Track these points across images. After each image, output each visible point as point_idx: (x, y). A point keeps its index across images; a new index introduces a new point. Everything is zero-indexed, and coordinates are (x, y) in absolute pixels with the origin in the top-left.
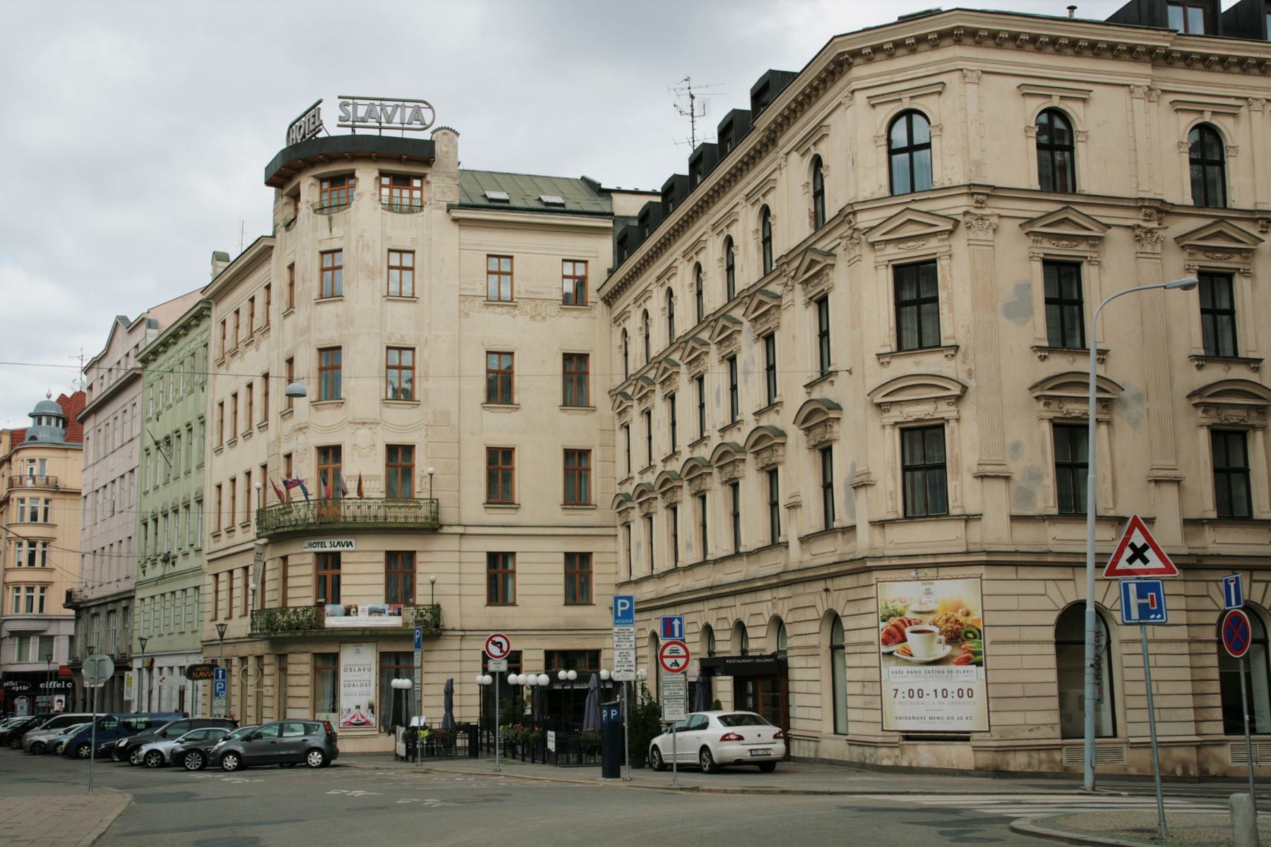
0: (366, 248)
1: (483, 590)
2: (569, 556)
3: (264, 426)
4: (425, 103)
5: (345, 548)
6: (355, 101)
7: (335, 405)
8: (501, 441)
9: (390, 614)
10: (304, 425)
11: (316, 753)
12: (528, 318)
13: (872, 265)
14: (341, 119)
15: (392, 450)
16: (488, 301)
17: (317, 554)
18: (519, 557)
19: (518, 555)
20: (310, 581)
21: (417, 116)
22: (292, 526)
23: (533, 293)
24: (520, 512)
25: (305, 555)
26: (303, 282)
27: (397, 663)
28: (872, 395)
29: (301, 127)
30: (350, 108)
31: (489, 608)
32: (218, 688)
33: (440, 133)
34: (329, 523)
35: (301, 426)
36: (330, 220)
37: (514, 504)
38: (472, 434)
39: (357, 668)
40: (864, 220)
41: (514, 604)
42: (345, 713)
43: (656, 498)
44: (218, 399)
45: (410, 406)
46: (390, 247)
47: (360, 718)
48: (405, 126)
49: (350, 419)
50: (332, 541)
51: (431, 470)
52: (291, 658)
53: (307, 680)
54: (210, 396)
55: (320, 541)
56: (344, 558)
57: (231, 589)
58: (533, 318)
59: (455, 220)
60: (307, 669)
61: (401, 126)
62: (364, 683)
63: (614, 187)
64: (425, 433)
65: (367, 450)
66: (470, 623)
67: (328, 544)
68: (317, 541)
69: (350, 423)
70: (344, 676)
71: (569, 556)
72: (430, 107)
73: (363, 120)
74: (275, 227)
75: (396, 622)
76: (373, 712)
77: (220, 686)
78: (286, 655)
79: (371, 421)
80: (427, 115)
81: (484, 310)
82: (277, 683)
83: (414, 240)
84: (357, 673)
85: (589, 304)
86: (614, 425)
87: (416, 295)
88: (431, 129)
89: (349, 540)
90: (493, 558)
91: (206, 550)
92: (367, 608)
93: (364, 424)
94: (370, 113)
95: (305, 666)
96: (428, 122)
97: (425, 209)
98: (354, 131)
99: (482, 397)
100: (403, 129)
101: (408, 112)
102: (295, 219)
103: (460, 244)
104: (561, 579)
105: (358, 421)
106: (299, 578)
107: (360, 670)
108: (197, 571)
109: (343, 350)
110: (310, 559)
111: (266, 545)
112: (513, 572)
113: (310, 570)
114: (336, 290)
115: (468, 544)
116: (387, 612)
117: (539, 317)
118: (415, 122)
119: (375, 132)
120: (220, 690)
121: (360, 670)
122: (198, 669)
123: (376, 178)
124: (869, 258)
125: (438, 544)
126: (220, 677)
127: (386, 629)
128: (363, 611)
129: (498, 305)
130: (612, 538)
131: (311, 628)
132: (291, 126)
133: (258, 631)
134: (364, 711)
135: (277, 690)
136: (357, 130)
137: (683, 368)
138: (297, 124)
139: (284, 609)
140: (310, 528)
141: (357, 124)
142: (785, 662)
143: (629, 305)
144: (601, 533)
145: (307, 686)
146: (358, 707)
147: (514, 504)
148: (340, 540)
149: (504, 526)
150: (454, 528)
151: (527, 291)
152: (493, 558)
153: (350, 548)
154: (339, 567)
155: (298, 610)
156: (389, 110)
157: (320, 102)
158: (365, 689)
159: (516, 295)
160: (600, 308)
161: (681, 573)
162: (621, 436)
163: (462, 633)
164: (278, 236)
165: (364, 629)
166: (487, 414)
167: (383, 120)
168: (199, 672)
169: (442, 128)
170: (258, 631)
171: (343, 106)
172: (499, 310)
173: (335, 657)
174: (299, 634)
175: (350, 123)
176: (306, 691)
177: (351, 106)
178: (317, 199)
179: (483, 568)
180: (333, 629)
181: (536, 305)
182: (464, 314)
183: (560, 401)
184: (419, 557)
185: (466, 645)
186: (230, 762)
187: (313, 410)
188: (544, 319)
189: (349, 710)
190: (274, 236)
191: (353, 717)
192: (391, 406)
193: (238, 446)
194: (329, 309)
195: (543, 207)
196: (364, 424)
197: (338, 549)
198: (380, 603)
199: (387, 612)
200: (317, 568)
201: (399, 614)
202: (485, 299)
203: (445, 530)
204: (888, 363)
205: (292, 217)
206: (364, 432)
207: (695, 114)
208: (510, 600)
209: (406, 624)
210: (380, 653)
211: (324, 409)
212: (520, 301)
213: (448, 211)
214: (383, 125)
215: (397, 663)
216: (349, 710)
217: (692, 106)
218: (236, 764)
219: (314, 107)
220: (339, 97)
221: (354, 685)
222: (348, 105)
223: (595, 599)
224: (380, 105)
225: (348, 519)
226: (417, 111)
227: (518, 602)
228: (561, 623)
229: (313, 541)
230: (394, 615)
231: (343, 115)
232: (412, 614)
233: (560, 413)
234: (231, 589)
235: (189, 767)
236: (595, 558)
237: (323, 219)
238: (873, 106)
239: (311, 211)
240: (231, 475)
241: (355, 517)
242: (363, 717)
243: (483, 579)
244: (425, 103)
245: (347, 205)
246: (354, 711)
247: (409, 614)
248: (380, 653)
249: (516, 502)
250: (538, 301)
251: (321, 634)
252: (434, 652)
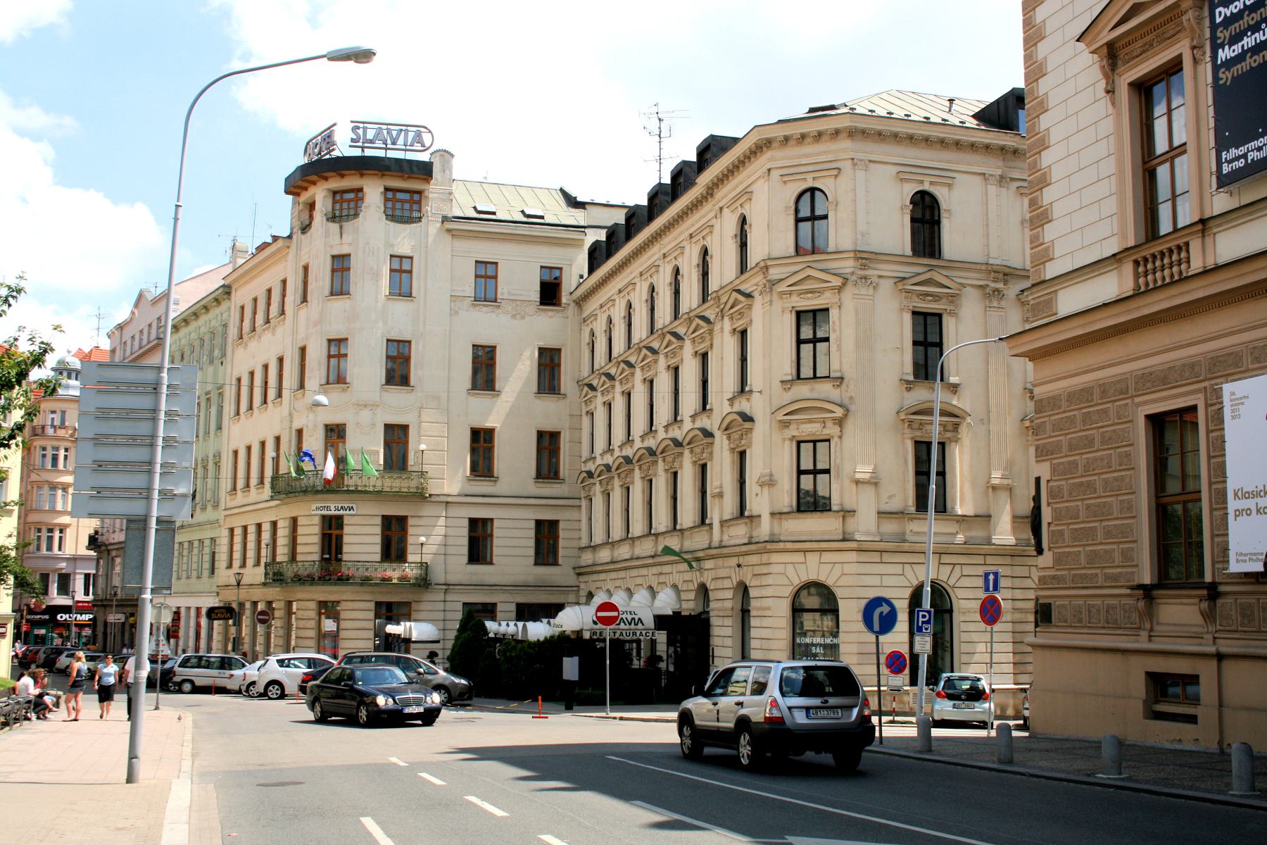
0: (371, 254)
1: (465, 550)
2: (539, 523)
4: (426, 128)
5: (348, 512)
6: (365, 125)
12: (509, 316)
13: (780, 310)
14: (353, 140)
15: (388, 427)
16: (475, 301)
17: (324, 517)
18: (496, 523)
19: (495, 521)
20: (316, 539)
21: (418, 138)
23: (513, 294)
24: (499, 484)
26: (316, 281)
28: (775, 414)
29: (317, 144)
30: (360, 132)
33: (438, 154)
36: (341, 227)
37: (493, 477)
40: (775, 273)
43: (614, 477)
44: (236, 375)
46: (392, 253)
48: (408, 148)
54: (229, 371)
58: (514, 316)
59: (449, 231)
61: (404, 147)
63: (588, 200)
66: (452, 579)
67: (333, 508)
69: (354, 404)
71: (539, 523)
72: (430, 132)
73: (371, 142)
74: (292, 229)
79: (372, 403)
80: (427, 138)
81: (472, 309)
83: (413, 247)
85: (563, 305)
86: (581, 411)
87: (413, 295)
88: (432, 150)
89: (351, 505)
90: (473, 523)
91: (222, 506)
93: (365, 406)
94: (377, 136)
96: (427, 145)
97: (423, 220)
98: (363, 151)
99: (467, 383)
100: (406, 150)
101: (411, 135)
102: (309, 225)
103: (452, 251)
104: (532, 543)
108: (214, 523)
109: (349, 342)
112: (491, 535)
114: (344, 288)
115: (454, 511)
117: (518, 316)
118: (416, 144)
119: (381, 153)
122: (216, 611)
123: (382, 193)
124: (778, 305)
125: (428, 510)
129: (484, 306)
132: (308, 143)
136: (365, 150)
137: (638, 373)
138: (314, 141)
141: (366, 145)
142: (708, 620)
143: (595, 309)
145: (313, 629)
147: (493, 477)
149: (484, 496)
151: (509, 293)
152: (473, 523)
153: (352, 512)
156: (394, 133)
157: (335, 125)
159: (499, 296)
160: (572, 308)
162: (586, 421)
163: (446, 587)
164: (295, 237)
167: (389, 142)
168: (217, 614)
169: (438, 151)
171: (355, 129)
172: (485, 309)
175: (360, 144)
177: (361, 130)
178: (330, 209)
181: (517, 305)
182: (454, 312)
183: (535, 389)
184: (411, 522)
185: (449, 598)
188: (523, 317)
190: (290, 237)
194: (339, 304)
195: (525, 220)
196: (365, 406)
197: (342, 512)
200: (323, 529)
202: (473, 299)
203: (433, 499)
204: (789, 388)
205: (307, 222)
206: (366, 415)
207: (662, 136)
208: (488, 559)
212: (503, 301)
213: (443, 222)
214: (388, 146)
217: (660, 128)
219: (329, 128)
220: (352, 122)
222: (358, 128)
223: (560, 561)
224: (387, 129)
226: (419, 134)
227: (494, 561)
228: (530, 580)
231: (355, 137)
236: (562, 525)
237: (334, 227)
238: (785, 182)
239: (325, 220)
240: (247, 442)
243: (465, 541)
244: (426, 128)
245: (356, 215)
249: (495, 475)
250: (518, 303)
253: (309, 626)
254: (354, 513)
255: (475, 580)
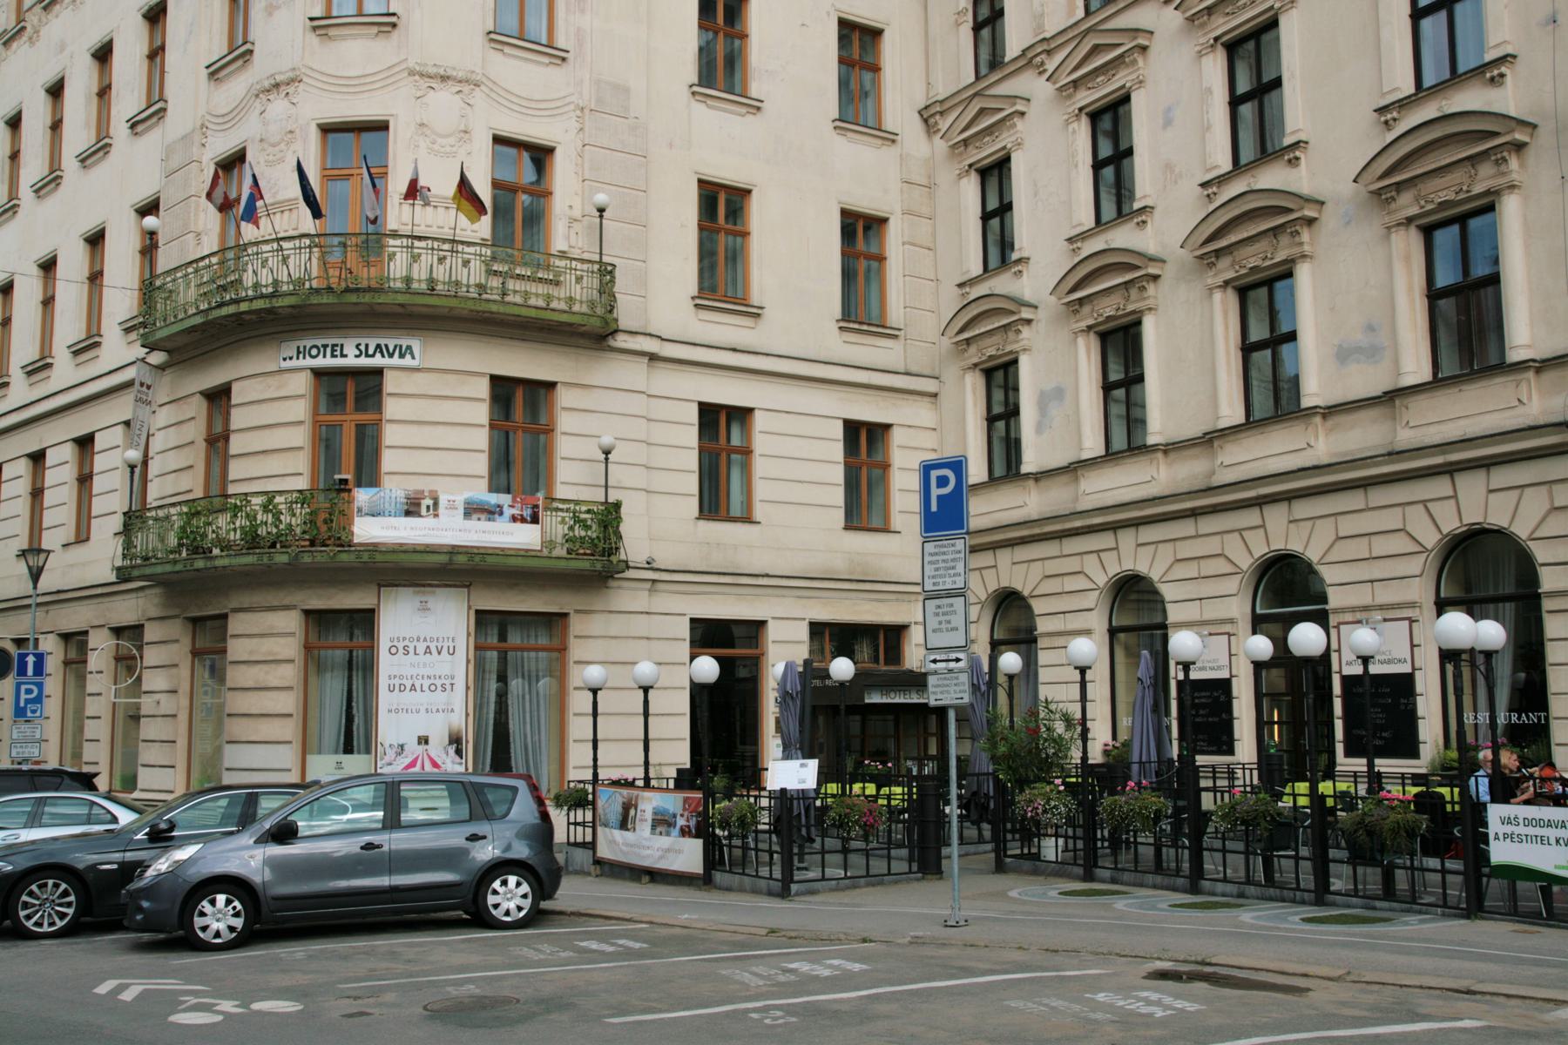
2: (852, 429)
3: (153, 112)
5: (396, 361)
7: (375, 29)
8: (727, 172)
9: (514, 519)
10: (291, 75)
11: (512, 880)
17: (318, 373)
20: (300, 437)
22: (263, 296)
24: (764, 324)
25: (287, 375)
27: (503, 637)
31: (702, 523)
32: (23, 697)
34: (369, 289)
35: (279, 78)
38: (671, 146)
39: (421, 647)
41: (747, 519)
42: (391, 754)
45: (546, 60)
47: (428, 767)
49: (411, 63)
50: (363, 341)
51: (601, 198)
52: (236, 624)
53: (289, 674)
55: (330, 342)
56: (391, 383)
57: (37, 493)
60: (290, 648)
62: (438, 683)
64: (578, 126)
65: (452, 140)
66: (665, 558)
67: (350, 350)
68: (319, 343)
69: (412, 73)
70: (387, 666)
71: (852, 429)
75: (525, 537)
76: (459, 752)
77: (29, 691)
78: (224, 617)
79: (461, 75)
82: (185, 687)
84: (422, 658)
92: (460, 499)
93: (444, 78)
95: (282, 640)
105: (433, 71)
106: (267, 432)
107: (428, 651)
110: (301, 384)
111: (161, 368)
112: (747, 452)
113: (300, 410)
116: (508, 512)
120: (27, 701)
121: (428, 651)
126: (30, 671)
127: (503, 553)
128: (452, 506)
130: (928, 399)
131: (313, 543)
133: (139, 561)
134: (439, 750)
135: (185, 702)
139: (218, 498)
140: (315, 300)
144: (912, 387)
145: (289, 688)
146: (424, 740)
148: (382, 342)
150: (640, 339)
152: (713, 418)
153: (408, 361)
154: (378, 407)
155: (279, 499)
158: (440, 698)
161: (1318, 419)
165: (454, 550)
166: (699, 109)
170: (139, 561)
173: (365, 621)
174: (281, 559)
176: (288, 703)
179: (690, 436)
180: (374, 548)
184: (564, 398)
186: (219, 916)
187: (313, 39)
189: (402, 747)
191: (413, 764)
192: (507, 50)
193: (62, 188)
196: (444, 78)
197: (378, 361)
198: (480, 491)
199: (508, 512)
201: (535, 519)
206: (444, 100)
208: (736, 510)
209: (549, 544)
210: (477, 612)
211: (343, 38)
215: (503, 637)
216: (402, 747)
218: (238, 923)
221: (413, 688)
225: (415, 286)
227: (759, 512)
228: (839, 566)
229: (309, 343)
230: (523, 520)
232: (563, 522)
233: (834, 133)
234: (37, 493)
235: (29, 924)
241: (431, 281)
242: (435, 765)
243: (692, 460)
246: (414, 749)
247: (556, 525)
248: (477, 612)
251: (344, 557)
252: (596, 616)
253: (275, 683)
254: (414, 363)
255: (717, 561)
